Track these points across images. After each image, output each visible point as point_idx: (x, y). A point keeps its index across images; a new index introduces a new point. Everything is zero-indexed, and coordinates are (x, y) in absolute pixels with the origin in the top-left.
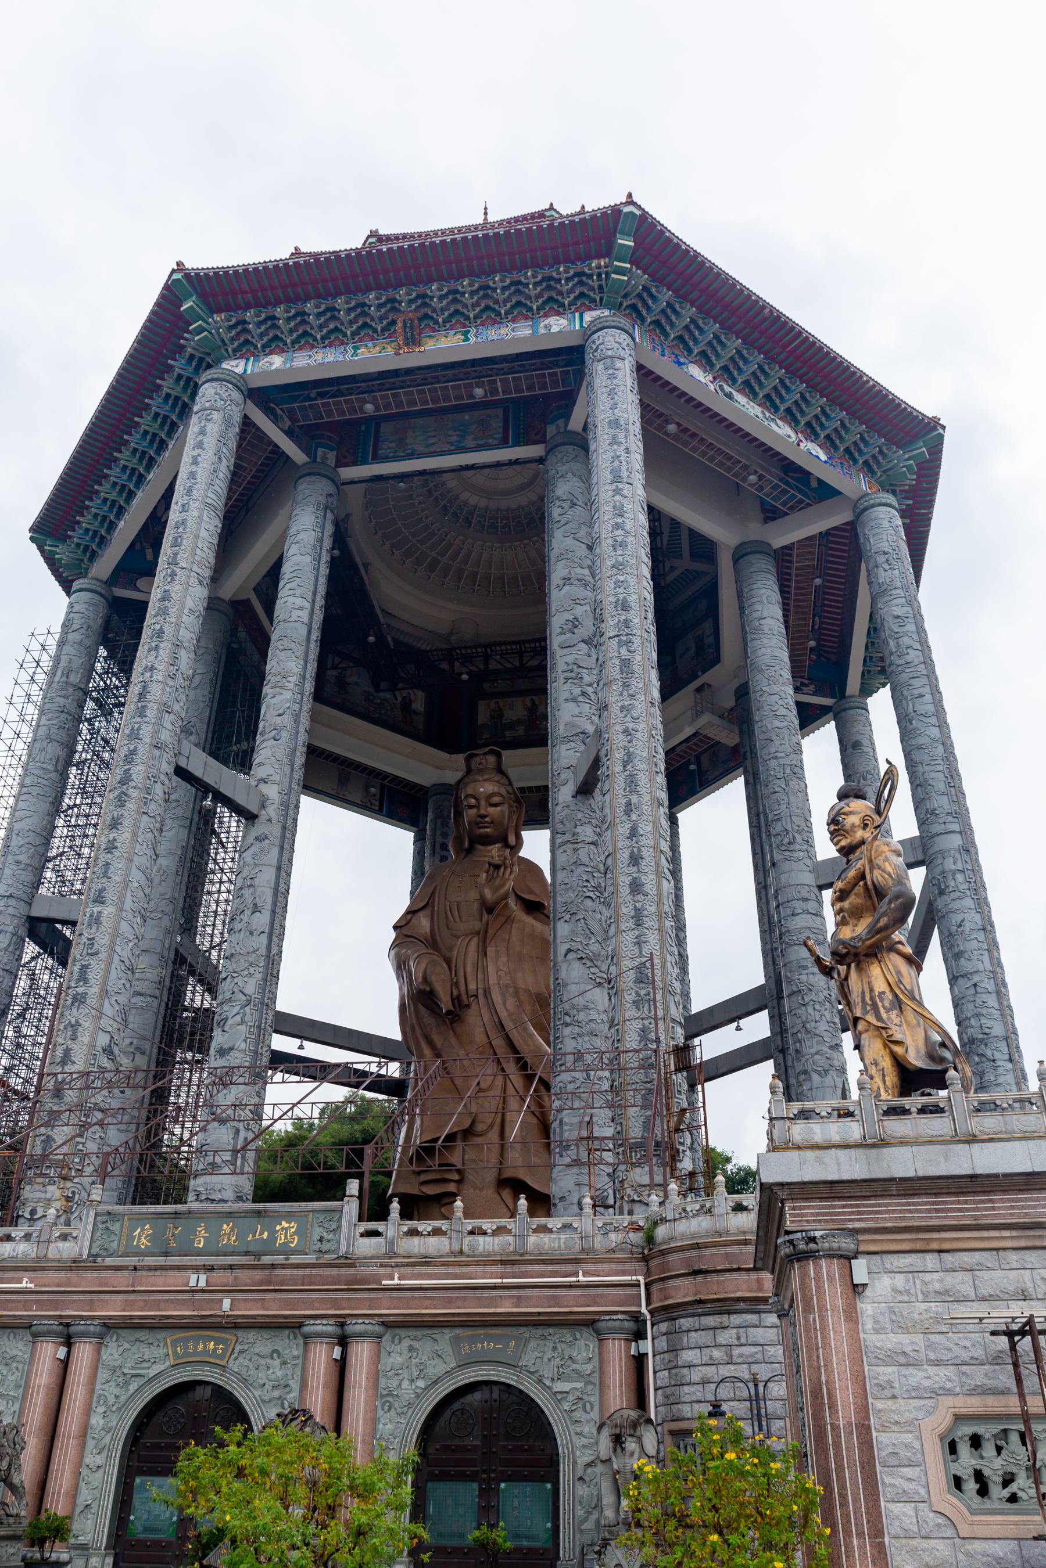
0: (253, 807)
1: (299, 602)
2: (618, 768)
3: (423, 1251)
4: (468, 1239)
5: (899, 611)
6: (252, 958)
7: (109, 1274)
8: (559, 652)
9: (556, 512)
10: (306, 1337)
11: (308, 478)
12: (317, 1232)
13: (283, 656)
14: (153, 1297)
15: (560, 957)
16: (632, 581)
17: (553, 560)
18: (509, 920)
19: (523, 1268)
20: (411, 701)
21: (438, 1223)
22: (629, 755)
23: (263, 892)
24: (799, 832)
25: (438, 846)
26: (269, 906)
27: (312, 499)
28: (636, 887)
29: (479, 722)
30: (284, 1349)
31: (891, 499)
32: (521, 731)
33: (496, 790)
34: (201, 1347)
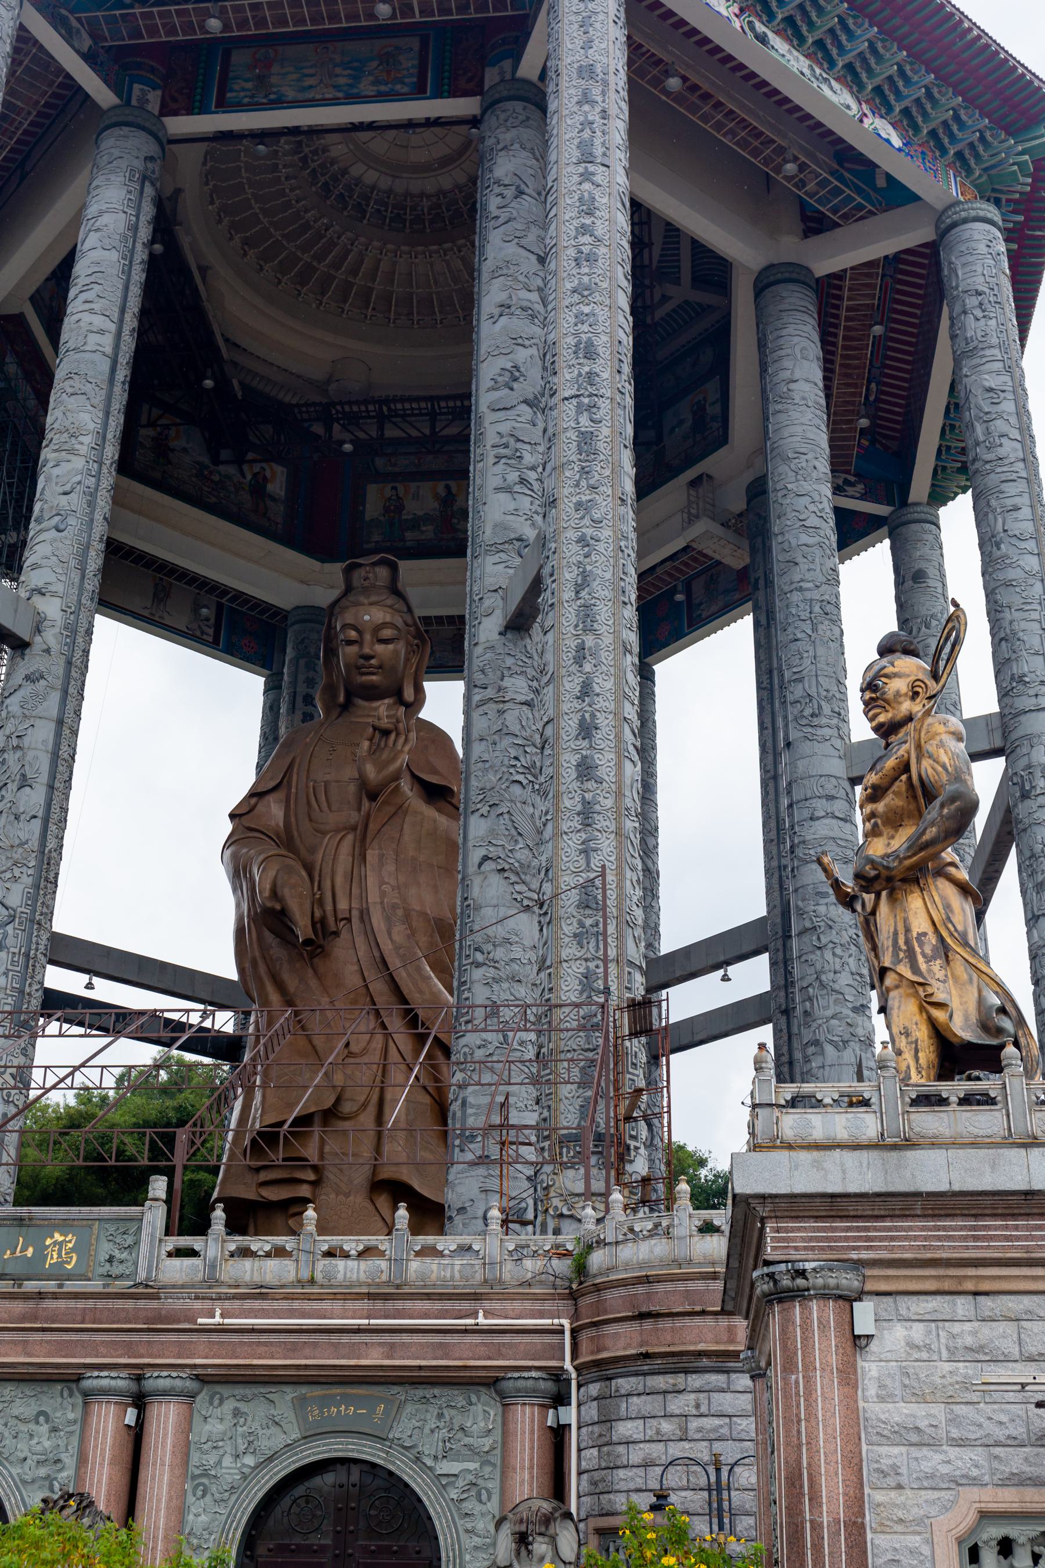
0: (23, 632)
1: (99, 321)
2: (568, 594)
3: (257, 1279)
4: (322, 1264)
5: (991, 382)
8: (489, 417)
9: (493, 203)
10: (86, 1394)
11: (116, 131)
12: (106, 1248)
13: (72, 403)
15: (472, 869)
16: (602, 314)
17: (485, 276)
18: (401, 810)
19: (399, 1305)
21: (279, 1240)
22: (585, 575)
23: (36, 758)
24: (828, 700)
25: (299, 700)
26: (44, 778)
27: (123, 164)
28: (586, 770)
29: (368, 516)
30: (55, 1410)
31: (992, 212)
32: (428, 532)
33: (388, 619)
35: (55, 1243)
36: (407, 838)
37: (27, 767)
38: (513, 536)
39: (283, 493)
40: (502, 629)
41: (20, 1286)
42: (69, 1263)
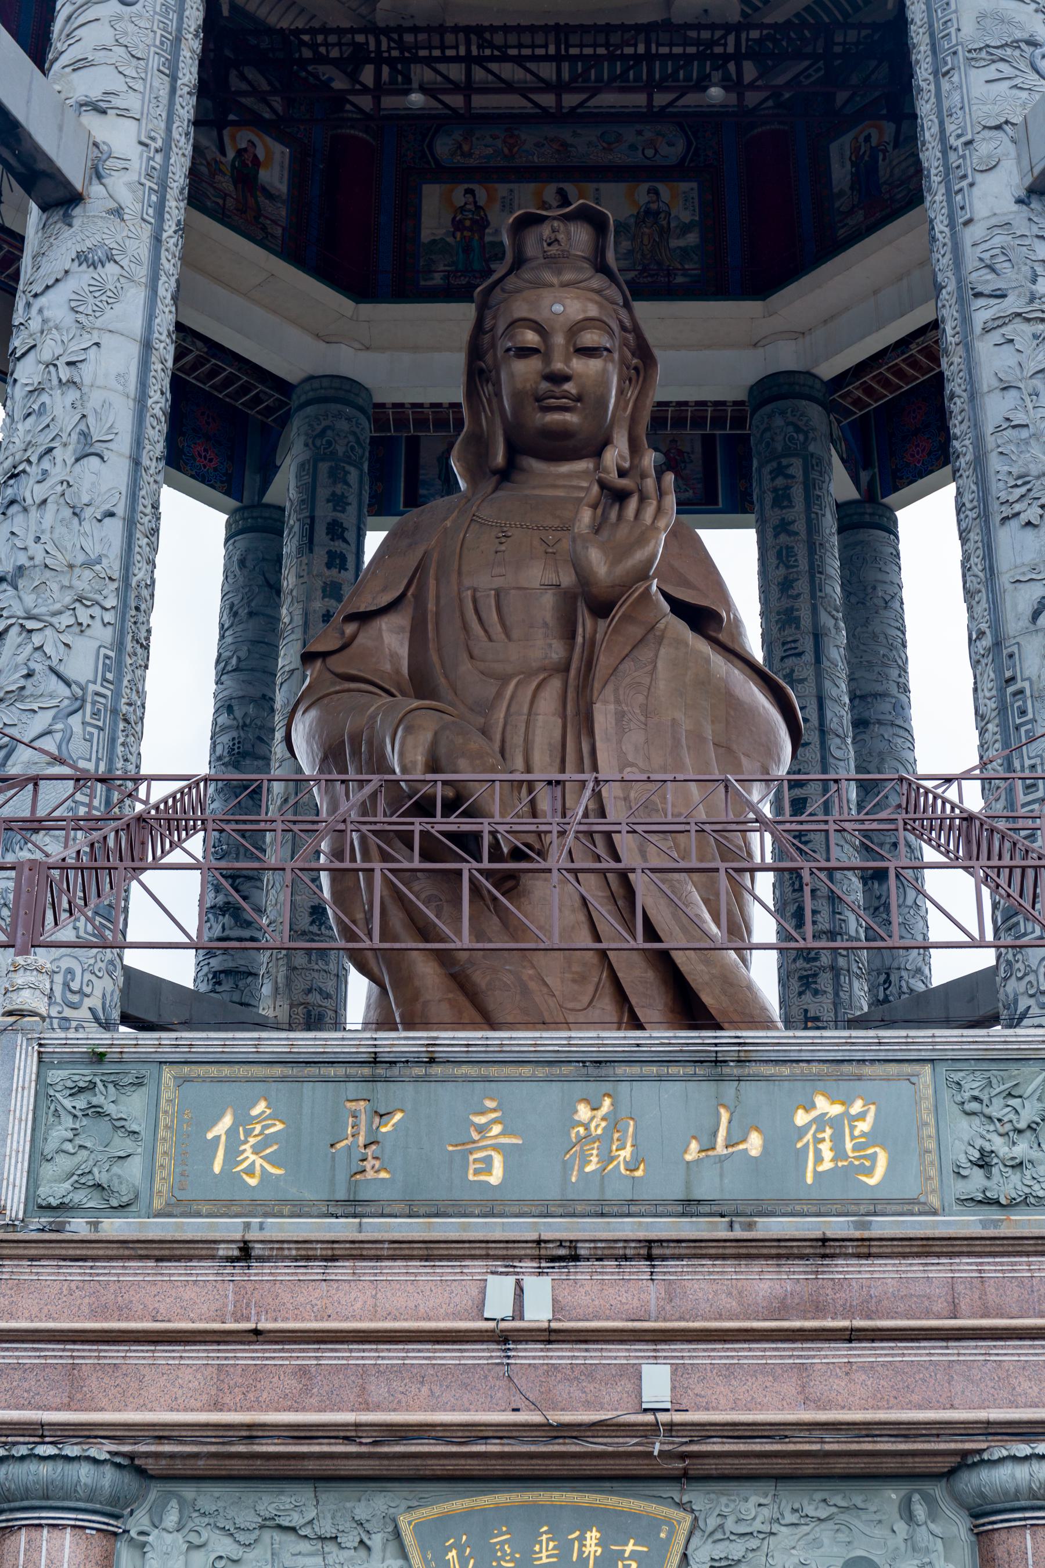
0: (75, 173)
6: (83, 582)
7: (136, 1273)
10: (983, 1516)
12: (964, 1136)
14: (334, 1356)
18: (651, 635)
20: (256, 162)
25: (320, 531)
26: (123, 444)
29: (426, 236)
33: (593, 311)
34: (545, 1551)
35: (821, 1121)
36: (662, 686)
37: (91, 420)
38: (1018, 35)
39: (284, 188)
40: (1022, 193)
41: (750, 1226)
42: (870, 1171)
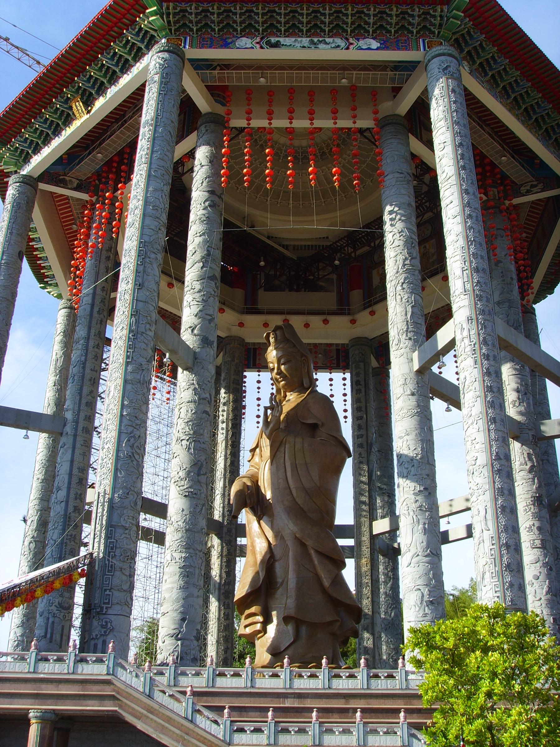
26: (66, 485)
